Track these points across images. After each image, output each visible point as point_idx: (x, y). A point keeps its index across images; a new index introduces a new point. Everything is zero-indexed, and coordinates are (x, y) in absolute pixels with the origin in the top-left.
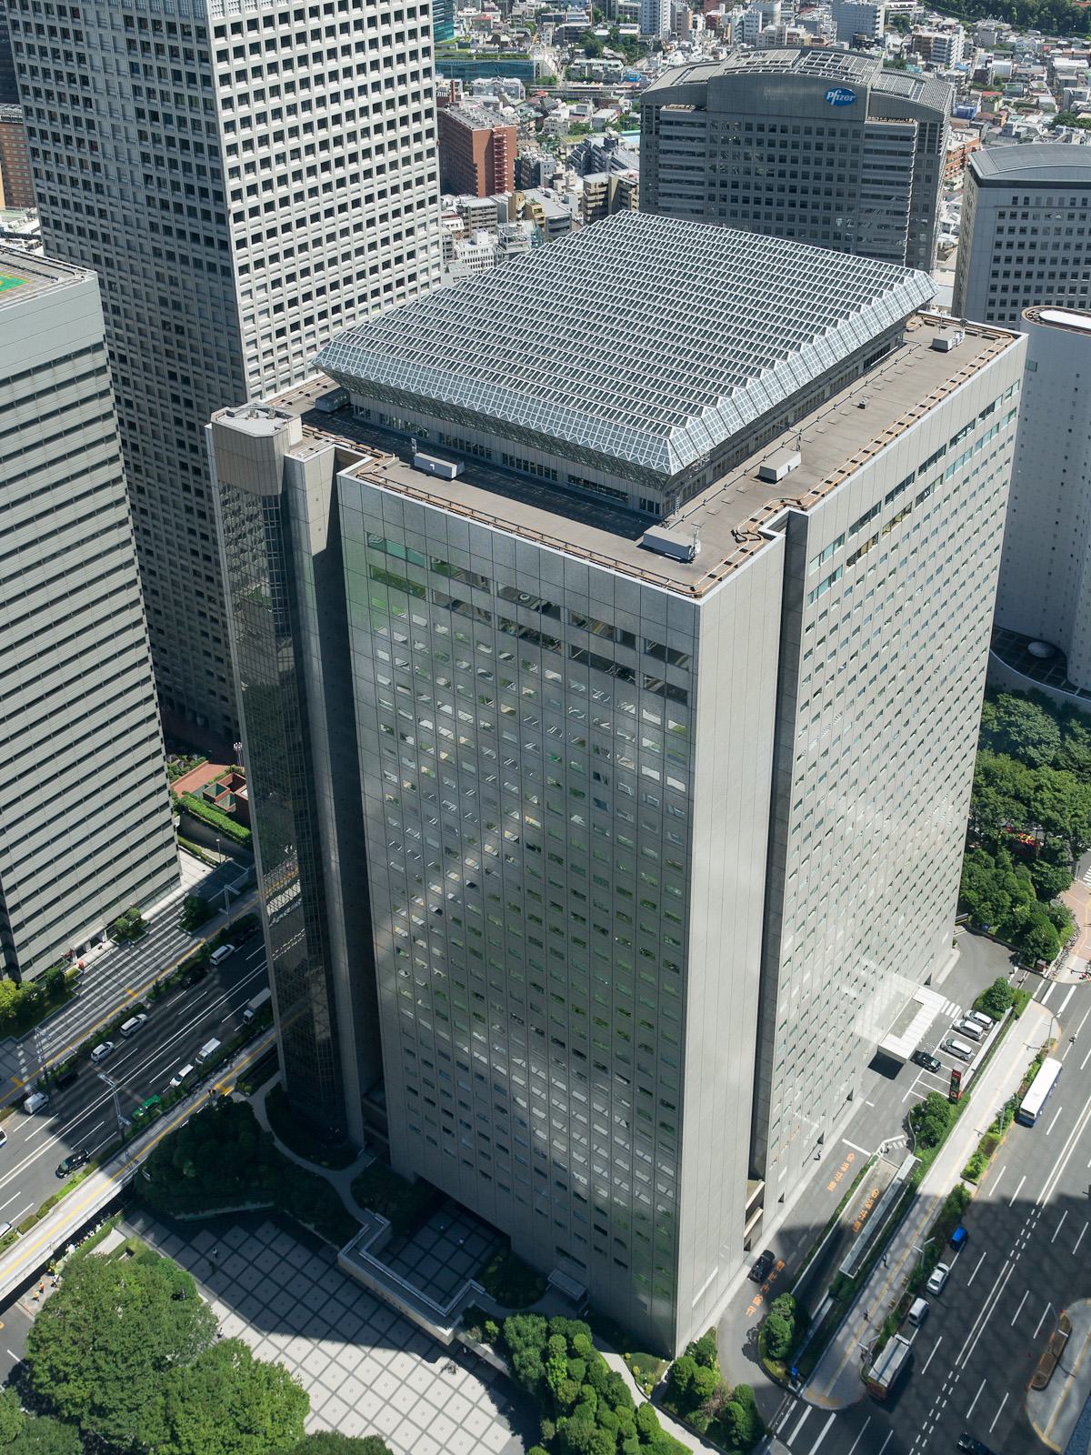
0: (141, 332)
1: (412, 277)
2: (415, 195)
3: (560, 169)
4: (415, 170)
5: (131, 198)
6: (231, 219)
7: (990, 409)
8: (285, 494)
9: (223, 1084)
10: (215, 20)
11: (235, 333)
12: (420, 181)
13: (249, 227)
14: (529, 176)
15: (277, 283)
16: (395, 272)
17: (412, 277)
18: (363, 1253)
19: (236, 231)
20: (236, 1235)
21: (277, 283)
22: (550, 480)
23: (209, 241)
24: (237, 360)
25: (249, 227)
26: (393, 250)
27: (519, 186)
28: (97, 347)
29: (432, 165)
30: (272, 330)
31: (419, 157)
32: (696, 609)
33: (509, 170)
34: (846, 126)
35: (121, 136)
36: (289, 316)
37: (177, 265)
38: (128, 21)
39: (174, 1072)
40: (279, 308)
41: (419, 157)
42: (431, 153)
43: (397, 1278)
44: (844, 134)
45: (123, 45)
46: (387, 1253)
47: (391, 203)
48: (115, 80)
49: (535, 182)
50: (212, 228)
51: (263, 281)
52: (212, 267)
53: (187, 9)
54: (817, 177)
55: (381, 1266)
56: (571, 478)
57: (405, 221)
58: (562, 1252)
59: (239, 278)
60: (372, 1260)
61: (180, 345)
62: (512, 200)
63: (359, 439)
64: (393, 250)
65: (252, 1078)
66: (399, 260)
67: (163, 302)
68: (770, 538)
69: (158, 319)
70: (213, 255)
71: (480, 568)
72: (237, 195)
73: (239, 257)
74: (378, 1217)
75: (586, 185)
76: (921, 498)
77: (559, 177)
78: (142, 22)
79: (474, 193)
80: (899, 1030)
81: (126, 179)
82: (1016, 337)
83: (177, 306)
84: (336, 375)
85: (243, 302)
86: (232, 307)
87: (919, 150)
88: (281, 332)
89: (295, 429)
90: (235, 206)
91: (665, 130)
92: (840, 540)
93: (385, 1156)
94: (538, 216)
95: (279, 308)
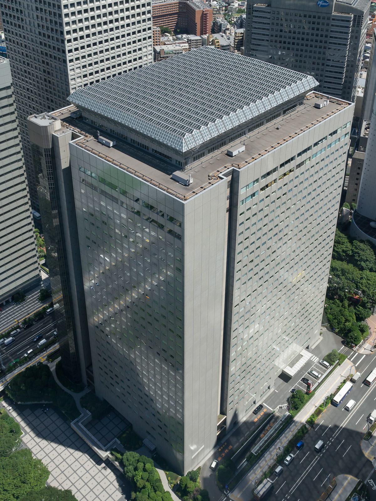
0: (38, 82)
2: (142, 35)
3: (229, 26)
5: (34, 32)
6: (66, 42)
7: (335, 132)
8: (53, 148)
9: (42, 358)
14: (217, 28)
15: (84, 67)
18: (80, 424)
19: (68, 46)
20: (39, 412)
21: (84, 67)
22: (146, 150)
26: (132, 56)
27: (213, 32)
28: (8, 88)
30: (83, 84)
32: (183, 204)
33: (210, 24)
34: (325, 15)
35: (30, 8)
39: (26, 352)
40: (85, 76)
43: (90, 434)
44: (324, 18)
46: (89, 425)
47: (132, 38)
51: (79, 65)
54: (317, 35)
55: (85, 429)
56: (153, 150)
57: (138, 45)
58: (148, 432)
59: (69, 64)
60: (82, 427)
61: (50, 88)
62: (208, 37)
63: (82, 129)
64: (132, 56)
65: (51, 357)
67: (44, 71)
68: (222, 179)
69: (43, 78)
71: (114, 182)
72: (68, 33)
73: (69, 56)
74: (88, 411)
75: (236, 33)
76: (299, 166)
77: (228, 29)
79: (195, 34)
80: (292, 365)
81: (32, 25)
82: (350, 104)
85: (70, 73)
86: (67, 75)
87: (353, 26)
89: (58, 125)
90: (67, 37)
91: (255, 14)
92: (257, 180)
93: (94, 390)
94: (217, 44)
95: (85, 76)
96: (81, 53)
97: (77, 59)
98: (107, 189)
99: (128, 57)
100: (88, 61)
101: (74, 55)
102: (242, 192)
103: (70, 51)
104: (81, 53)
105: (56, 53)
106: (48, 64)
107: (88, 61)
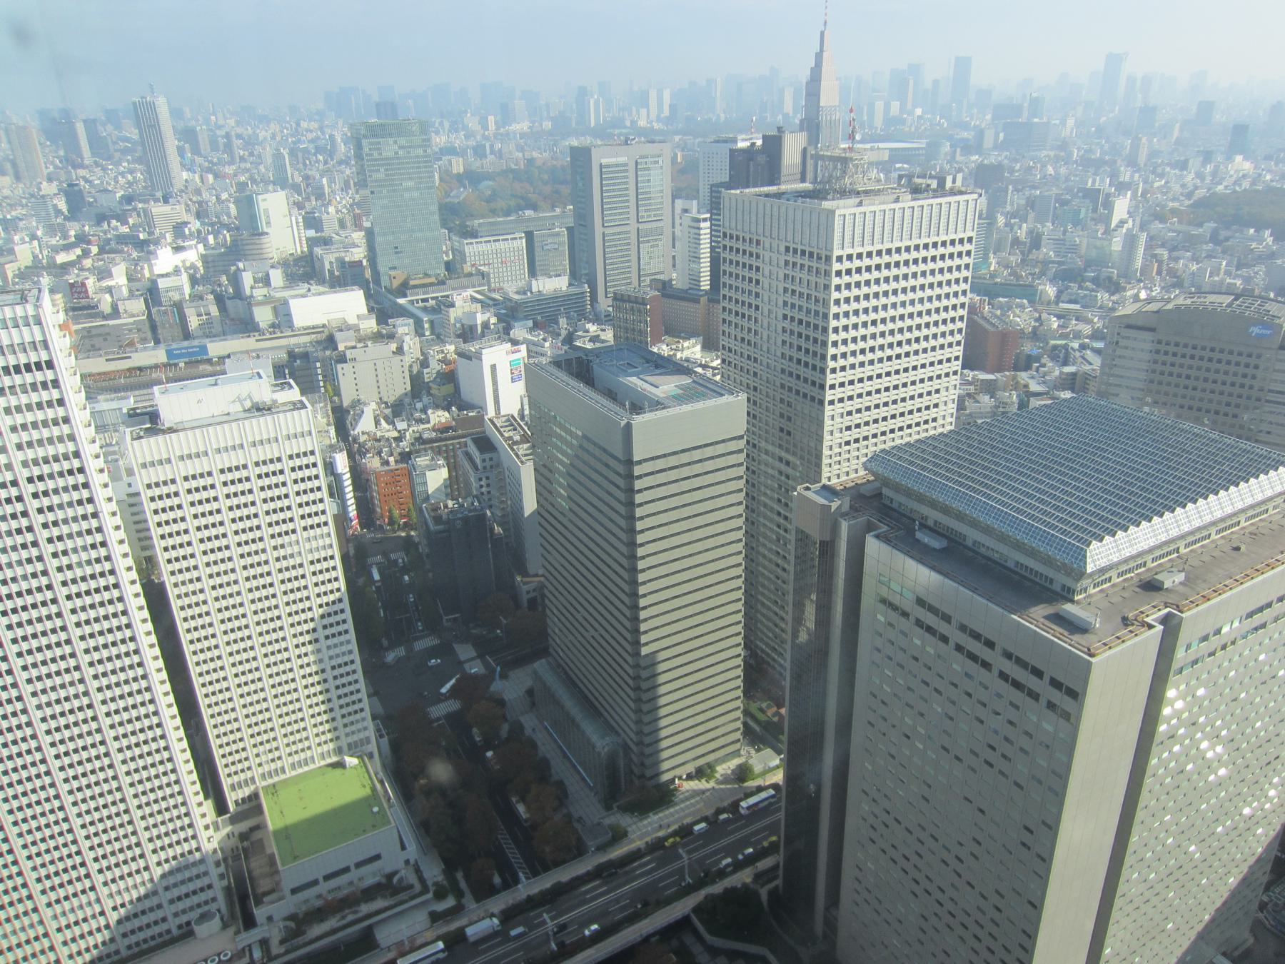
1: (934, 420)
2: (946, 368)
4: (947, 353)
10: (837, 252)
11: (820, 439)
12: (949, 360)
13: (840, 377)
14: (1026, 363)
15: (849, 413)
16: (925, 415)
17: (934, 420)
19: (830, 379)
21: (849, 413)
23: (814, 383)
24: (819, 456)
25: (840, 377)
29: (958, 351)
31: (950, 345)
32: (1090, 663)
36: (855, 434)
37: (793, 395)
38: (787, 249)
40: (849, 428)
41: (950, 345)
42: (958, 343)
45: (782, 263)
47: (929, 372)
48: (774, 283)
49: (1027, 368)
50: (816, 376)
52: (813, 399)
53: (822, 245)
57: (936, 384)
66: (927, 408)
68: (1150, 627)
70: (814, 392)
78: (795, 251)
83: (789, 419)
84: (873, 474)
85: (827, 422)
88: (848, 443)
92: (1205, 638)
95: (849, 428)
96: (849, 391)
97: (841, 400)
98: (930, 619)
99: (918, 403)
100: (857, 404)
101: (839, 393)
102: (1180, 653)
103: (832, 387)
104: (849, 391)
105: (807, 389)
106: (789, 405)
107: (857, 404)
